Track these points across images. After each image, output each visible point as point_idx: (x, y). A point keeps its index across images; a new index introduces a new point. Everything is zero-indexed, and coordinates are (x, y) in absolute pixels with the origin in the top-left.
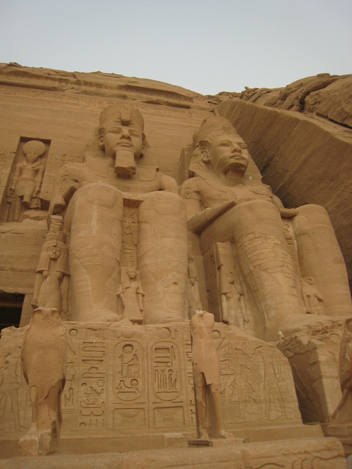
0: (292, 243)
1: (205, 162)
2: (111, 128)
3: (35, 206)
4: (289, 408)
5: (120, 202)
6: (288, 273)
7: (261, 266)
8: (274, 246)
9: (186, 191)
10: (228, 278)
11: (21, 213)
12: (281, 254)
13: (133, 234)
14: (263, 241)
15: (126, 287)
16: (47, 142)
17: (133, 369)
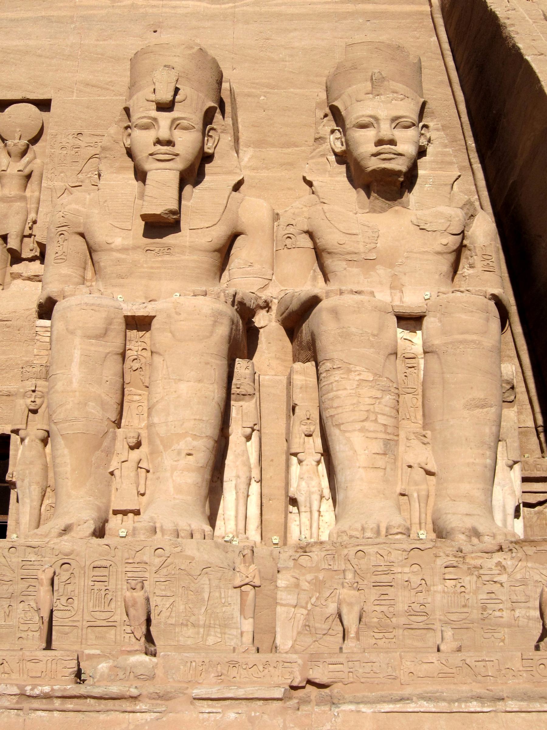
0: (414, 365)
1: (336, 154)
2: (139, 118)
3: (30, 255)
4: (229, 634)
5: (119, 325)
6: (374, 431)
7: (334, 419)
8: (358, 385)
9: (287, 232)
10: (304, 428)
11: (6, 267)
12: (367, 399)
13: (143, 368)
14: (343, 376)
15: (123, 460)
16: (44, 105)
17: (70, 588)
